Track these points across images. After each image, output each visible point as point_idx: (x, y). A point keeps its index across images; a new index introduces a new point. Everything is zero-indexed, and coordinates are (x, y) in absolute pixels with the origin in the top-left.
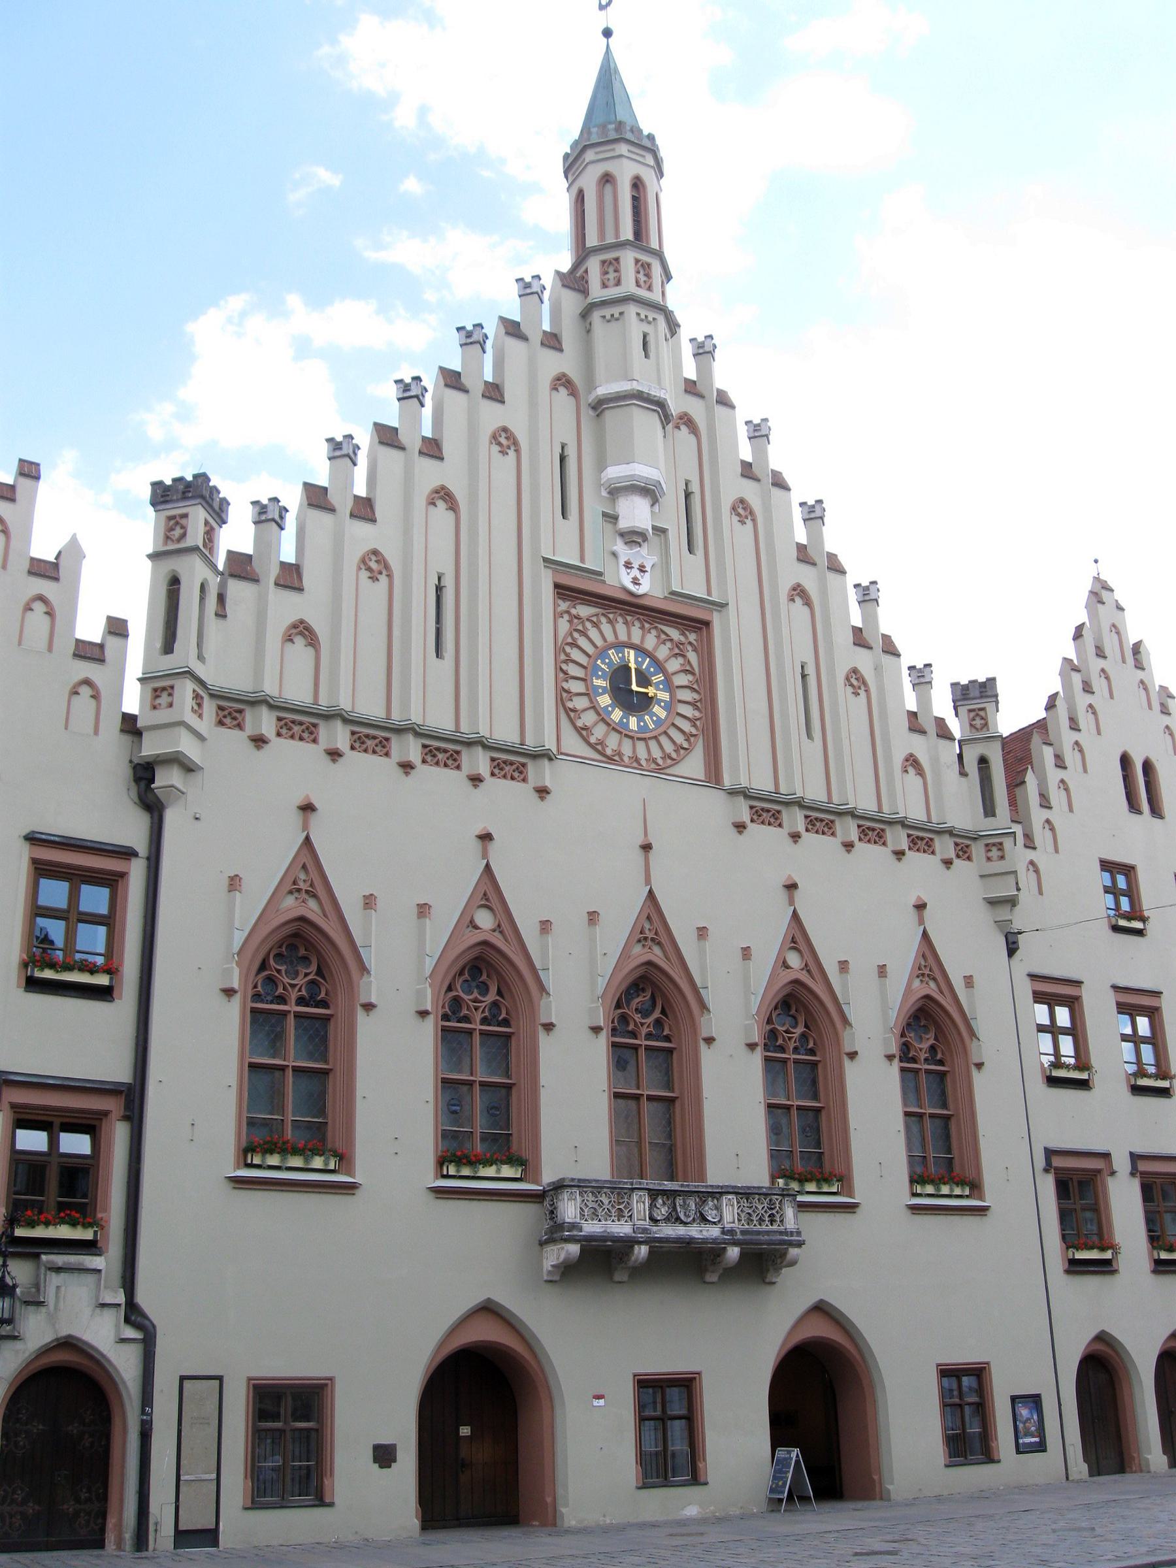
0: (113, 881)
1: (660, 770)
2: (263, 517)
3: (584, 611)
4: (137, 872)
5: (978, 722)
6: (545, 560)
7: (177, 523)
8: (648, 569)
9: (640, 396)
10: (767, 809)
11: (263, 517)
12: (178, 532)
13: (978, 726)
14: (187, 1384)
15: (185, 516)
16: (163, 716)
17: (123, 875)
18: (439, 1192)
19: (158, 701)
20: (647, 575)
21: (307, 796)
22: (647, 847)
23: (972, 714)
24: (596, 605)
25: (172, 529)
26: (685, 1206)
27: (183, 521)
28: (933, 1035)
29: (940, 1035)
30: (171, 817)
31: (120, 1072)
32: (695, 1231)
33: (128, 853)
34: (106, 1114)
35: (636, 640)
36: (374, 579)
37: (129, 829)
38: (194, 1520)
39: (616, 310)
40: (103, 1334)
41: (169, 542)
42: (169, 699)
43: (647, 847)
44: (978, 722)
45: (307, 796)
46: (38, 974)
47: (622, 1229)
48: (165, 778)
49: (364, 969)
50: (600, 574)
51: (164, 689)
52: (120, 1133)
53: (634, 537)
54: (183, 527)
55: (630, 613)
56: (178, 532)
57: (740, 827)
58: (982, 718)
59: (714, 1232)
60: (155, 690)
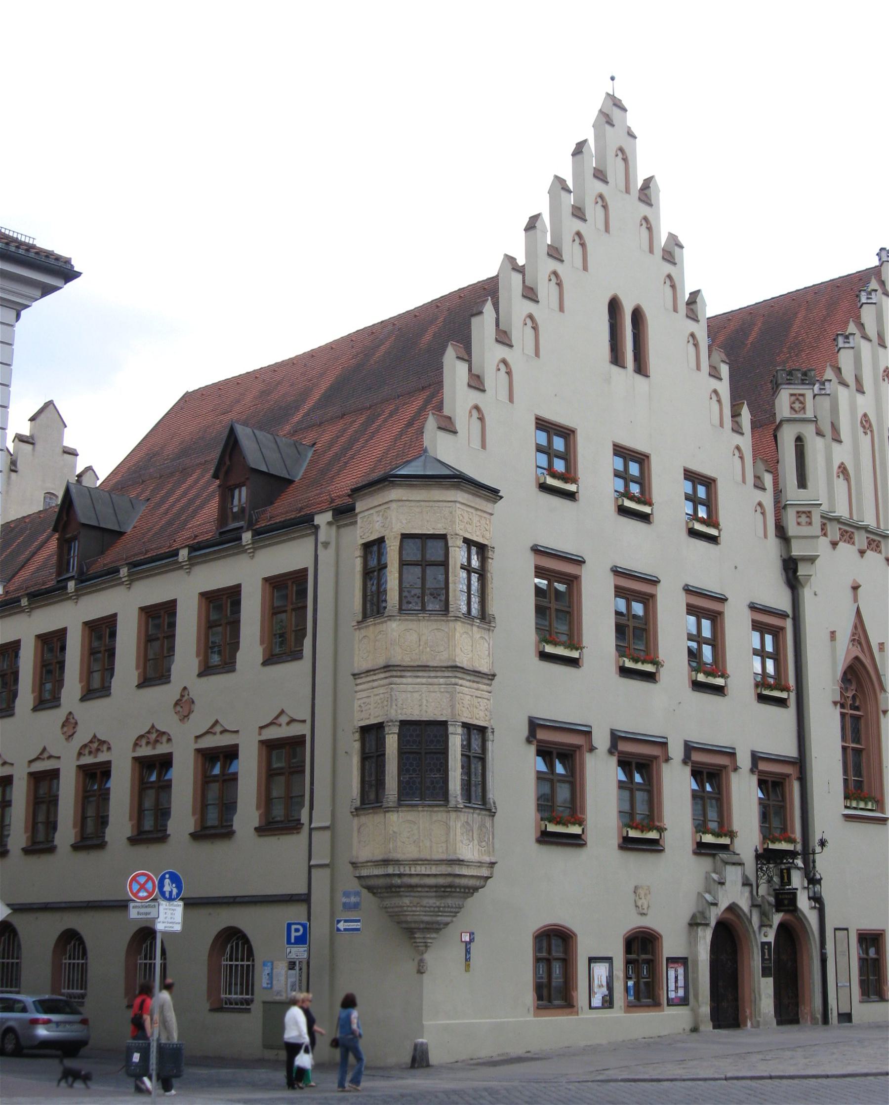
0: (777, 633)
2: (823, 392)
4: (789, 624)
7: (798, 399)
11: (823, 392)
14: (837, 932)
15: (803, 395)
16: (805, 531)
17: (783, 629)
18: (847, 817)
19: (800, 520)
21: (854, 580)
25: (794, 403)
27: (801, 398)
29: (860, 687)
30: (807, 594)
31: (790, 750)
33: (783, 615)
34: (788, 776)
36: (866, 433)
37: (780, 600)
38: (845, 1009)
41: (793, 412)
42: (808, 520)
45: (854, 580)
46: (766, 692)
48: (802, 570)
49: (883, 689)
51: (804, 512)
52: (796, 786)
54: (801, 403)
60: (798, 512)
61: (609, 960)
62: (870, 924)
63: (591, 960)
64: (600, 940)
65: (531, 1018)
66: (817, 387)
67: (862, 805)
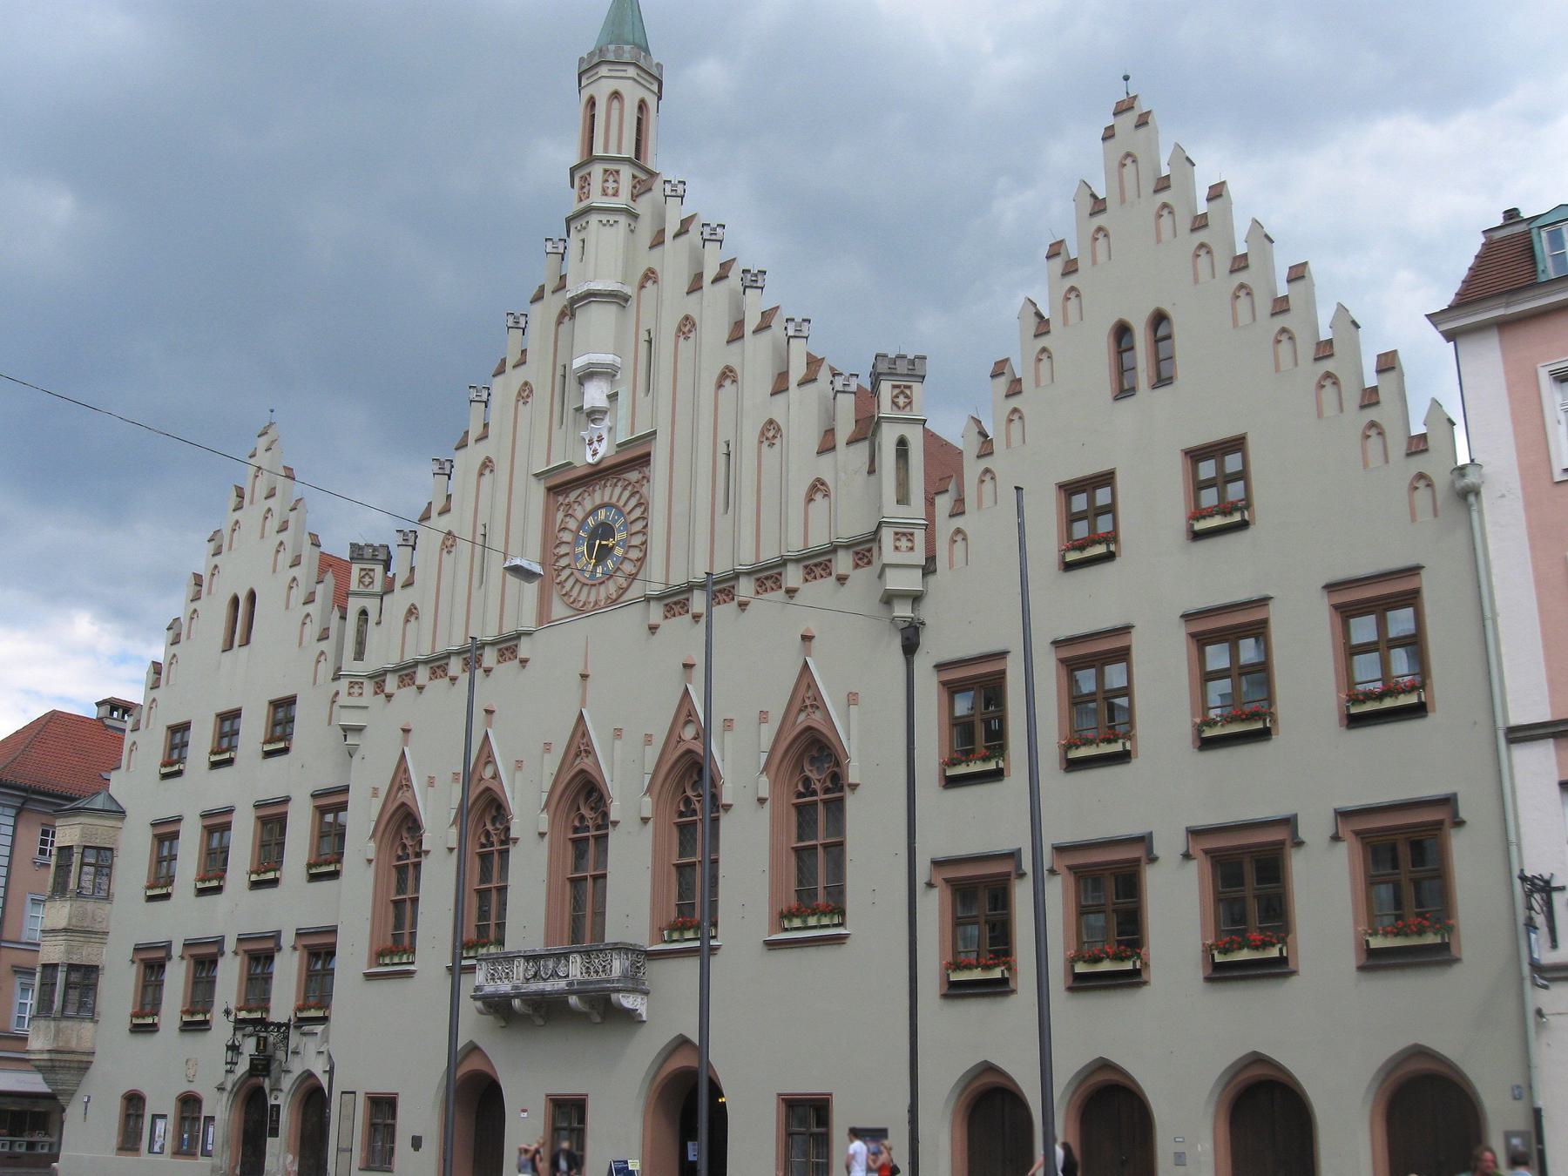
1: (614, 602)
3: (573, 496)
5: (901, 401)
6: (536, 475)
8: (605, 436)
9: (590, 296)
10: (675, 600)
12: (367, 580)
13: (901, 404)
20: (605, 442)
22: (584, 677)
23: (896, 391)
24: (577, 487)
26: (546, 967)
28: (812, 765)
32: (548, 986)
35: (598, 502)
39: (612, 218)
40: (319, 1068)
43: (584, 677)
44: (901, 401)
47: (505, 987)
50: (569, 464)
53: (594, 415)
55: (600, 479)
56: (367, 580)
57: (653, 629)
58: (907, 397)
59: (561, 985)
61: (164, 1116)
62: (382, 1087)
63: (155, 1117)
64: (162, 1101)
65: (113, 1156)
66: (854, 388)
67: (396, 960)
